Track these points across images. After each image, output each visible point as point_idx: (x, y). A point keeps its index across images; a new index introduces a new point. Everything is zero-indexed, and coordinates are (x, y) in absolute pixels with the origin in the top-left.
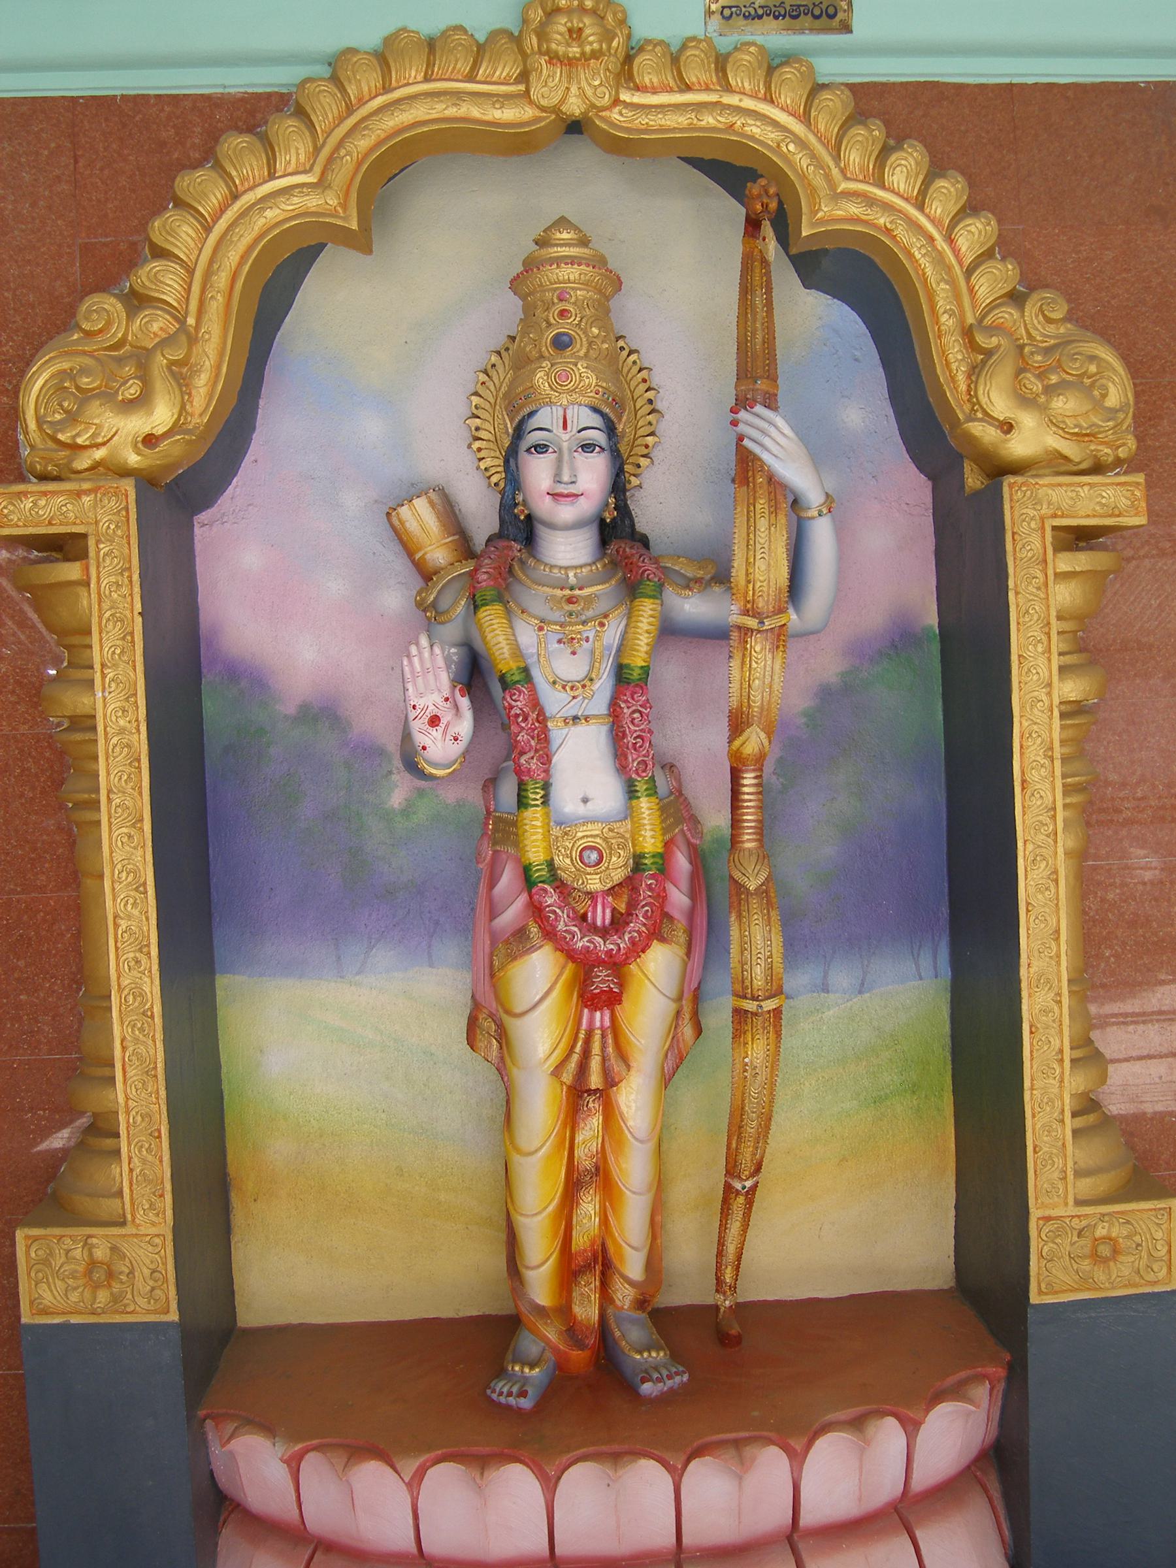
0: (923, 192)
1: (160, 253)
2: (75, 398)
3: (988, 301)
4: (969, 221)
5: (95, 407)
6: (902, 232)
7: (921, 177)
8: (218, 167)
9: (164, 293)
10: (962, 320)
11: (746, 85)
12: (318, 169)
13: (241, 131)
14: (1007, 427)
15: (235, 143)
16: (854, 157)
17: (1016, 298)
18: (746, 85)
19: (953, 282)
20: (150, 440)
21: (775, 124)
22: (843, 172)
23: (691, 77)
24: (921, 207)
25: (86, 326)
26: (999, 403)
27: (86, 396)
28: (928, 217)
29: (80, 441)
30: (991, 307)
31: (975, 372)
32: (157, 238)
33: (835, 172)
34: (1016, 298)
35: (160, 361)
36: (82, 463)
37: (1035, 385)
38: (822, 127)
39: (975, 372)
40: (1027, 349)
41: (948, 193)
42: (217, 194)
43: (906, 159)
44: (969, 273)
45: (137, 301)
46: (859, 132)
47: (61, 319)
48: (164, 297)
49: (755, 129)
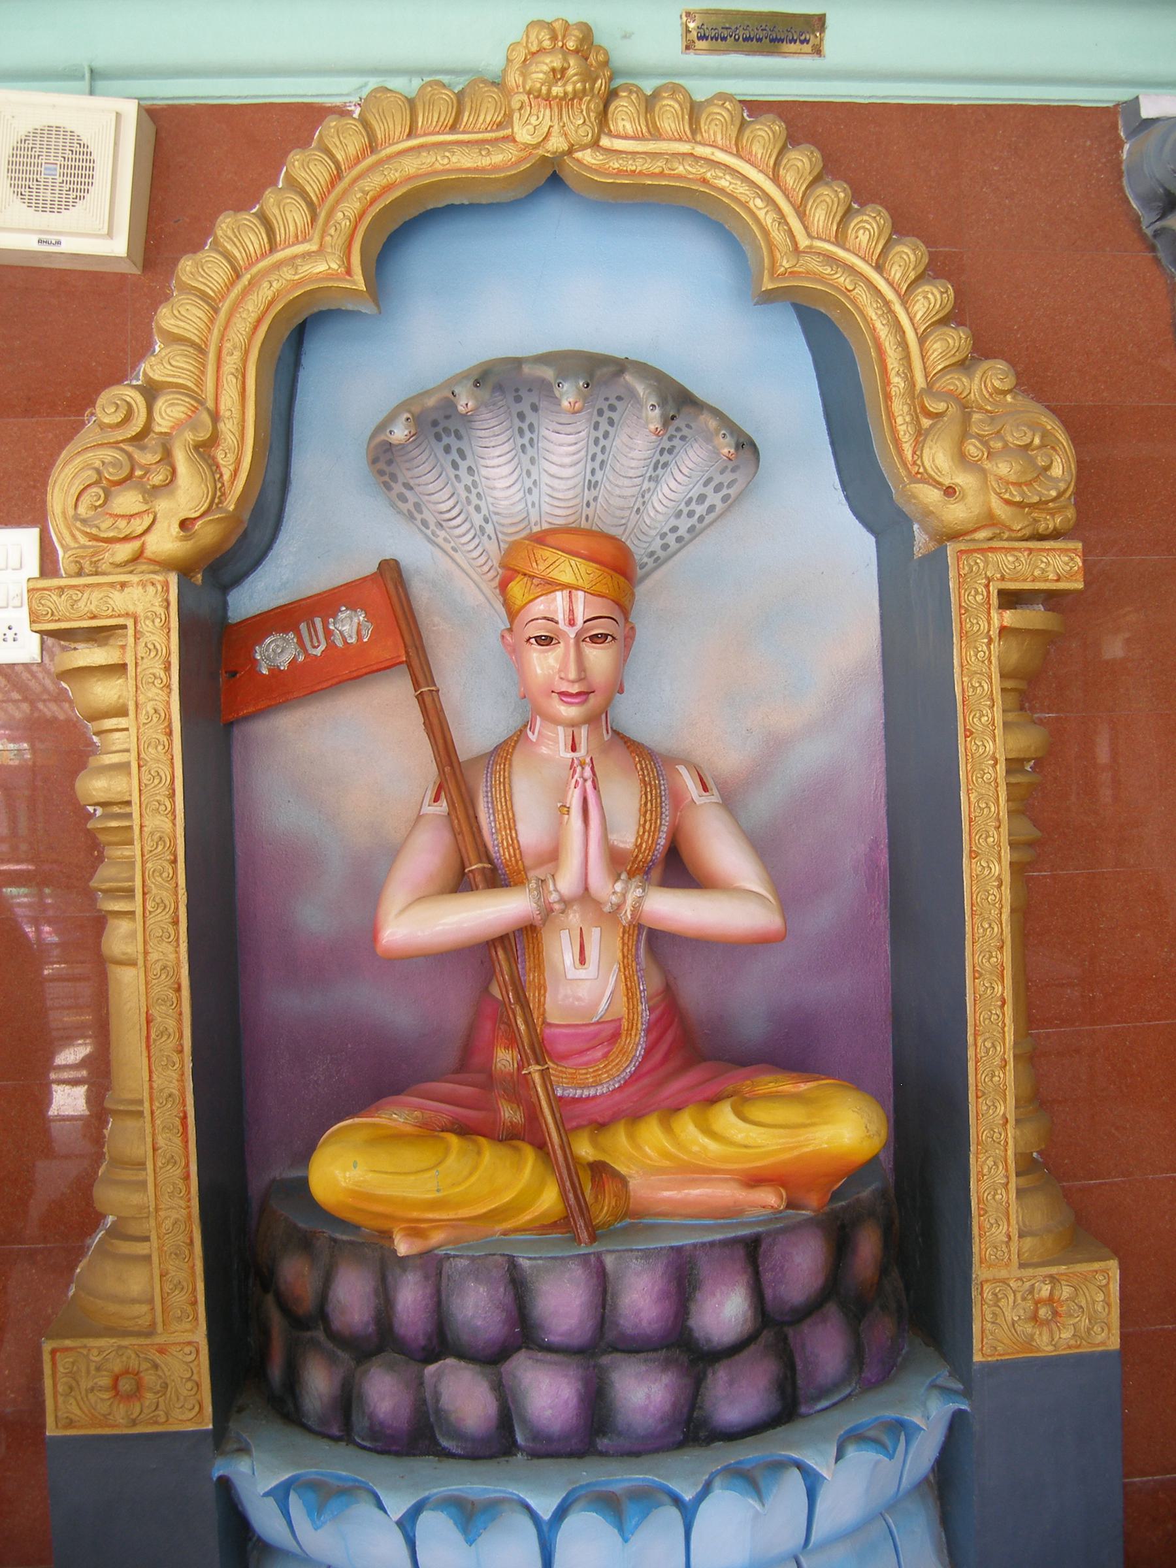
3: (940, 367)
4: (927, 288)
6: (862, 295)
10: (912, 384)
11: (719, 137)
12: (316, 238)
14: (950, 491)
16: (819, 216)
17: (964, 365)
19: (903, 344)
20: (184, 524)
21: (745, 179)
23: (667, 124)
24: (879, 268)
28: (887, 280)
31: (921, 436)
34: (964, 365)
39: (921, 436)
41: (907, 257)
43: (866, 221)
48: (181, 381)
49: (725, 182)
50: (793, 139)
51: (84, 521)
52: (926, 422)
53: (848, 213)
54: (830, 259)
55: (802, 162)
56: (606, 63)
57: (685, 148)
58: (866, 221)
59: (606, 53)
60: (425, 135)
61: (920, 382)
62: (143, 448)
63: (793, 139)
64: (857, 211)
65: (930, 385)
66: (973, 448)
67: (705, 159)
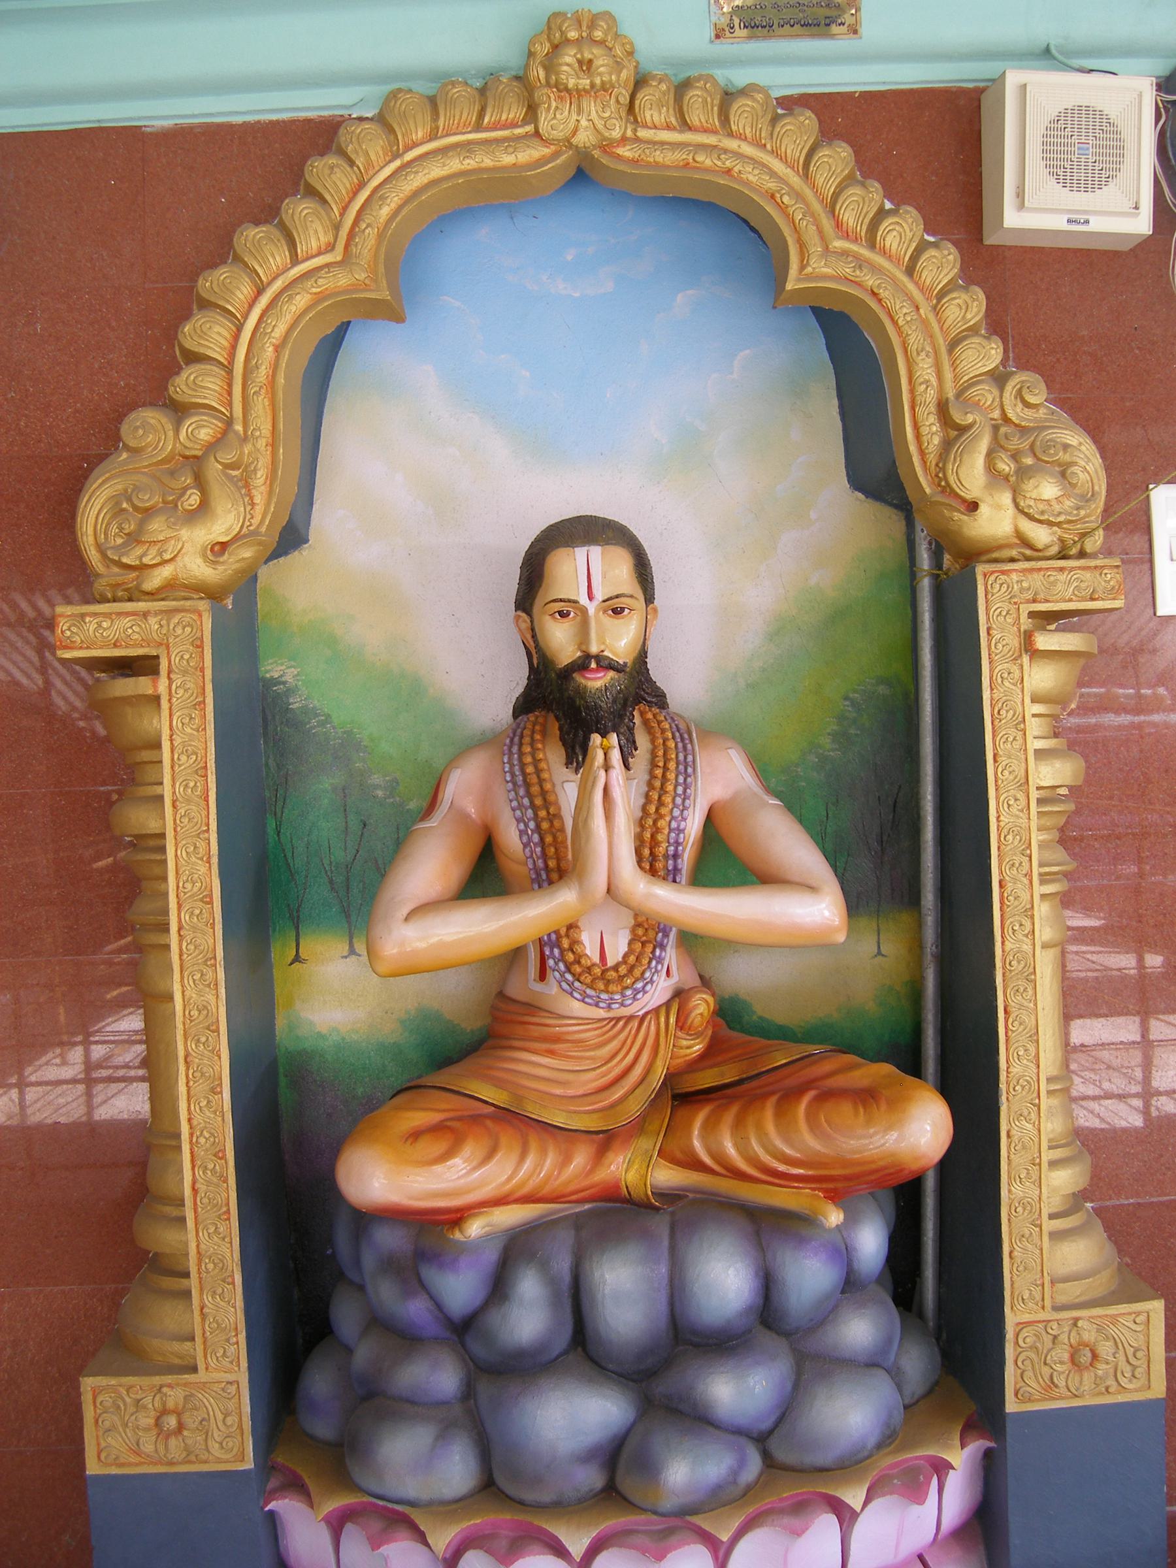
0: (915, 258)
1: (194, 358)
2: (135, 517)
5: (157, 527)
7: (914, 245)
8: (238, 259)
9: (205, 398)
11: (748, 130)
13: (257, 223)
15: (251, 235)
18: (748, 130)
22: (838, 225)
25: (132, 443)
26: (971, 474)
27: (148, 513)
28: (917, 284)
29: (146, 560)
30: (972, 384)
32: (189, 344)
33: (827, 224)
35: (213, 469)
36: (155, 580)
37: (1005, 465)
38: (820, 181)
40: (1003, 430)
42: (245, 290)
44: (953, 345)
45: (179, 410)
46: (855, 192)
47: (108, 439)
50: (828, 134)
51: (116, 548)
52: (954, 433)
53: (881, 214)
54: (860, 262)
55: (837, 159)
56: (631, 54)
57: (711, 140)
58: (898, 223)
59: (631, 44)
60: (447, 135)
61: (951, 394)
62: (172, 473)
63: (828, 134)
64: (890, 212)
65: (958, 395)
66: (1005, 465)
67: (732, 152)
